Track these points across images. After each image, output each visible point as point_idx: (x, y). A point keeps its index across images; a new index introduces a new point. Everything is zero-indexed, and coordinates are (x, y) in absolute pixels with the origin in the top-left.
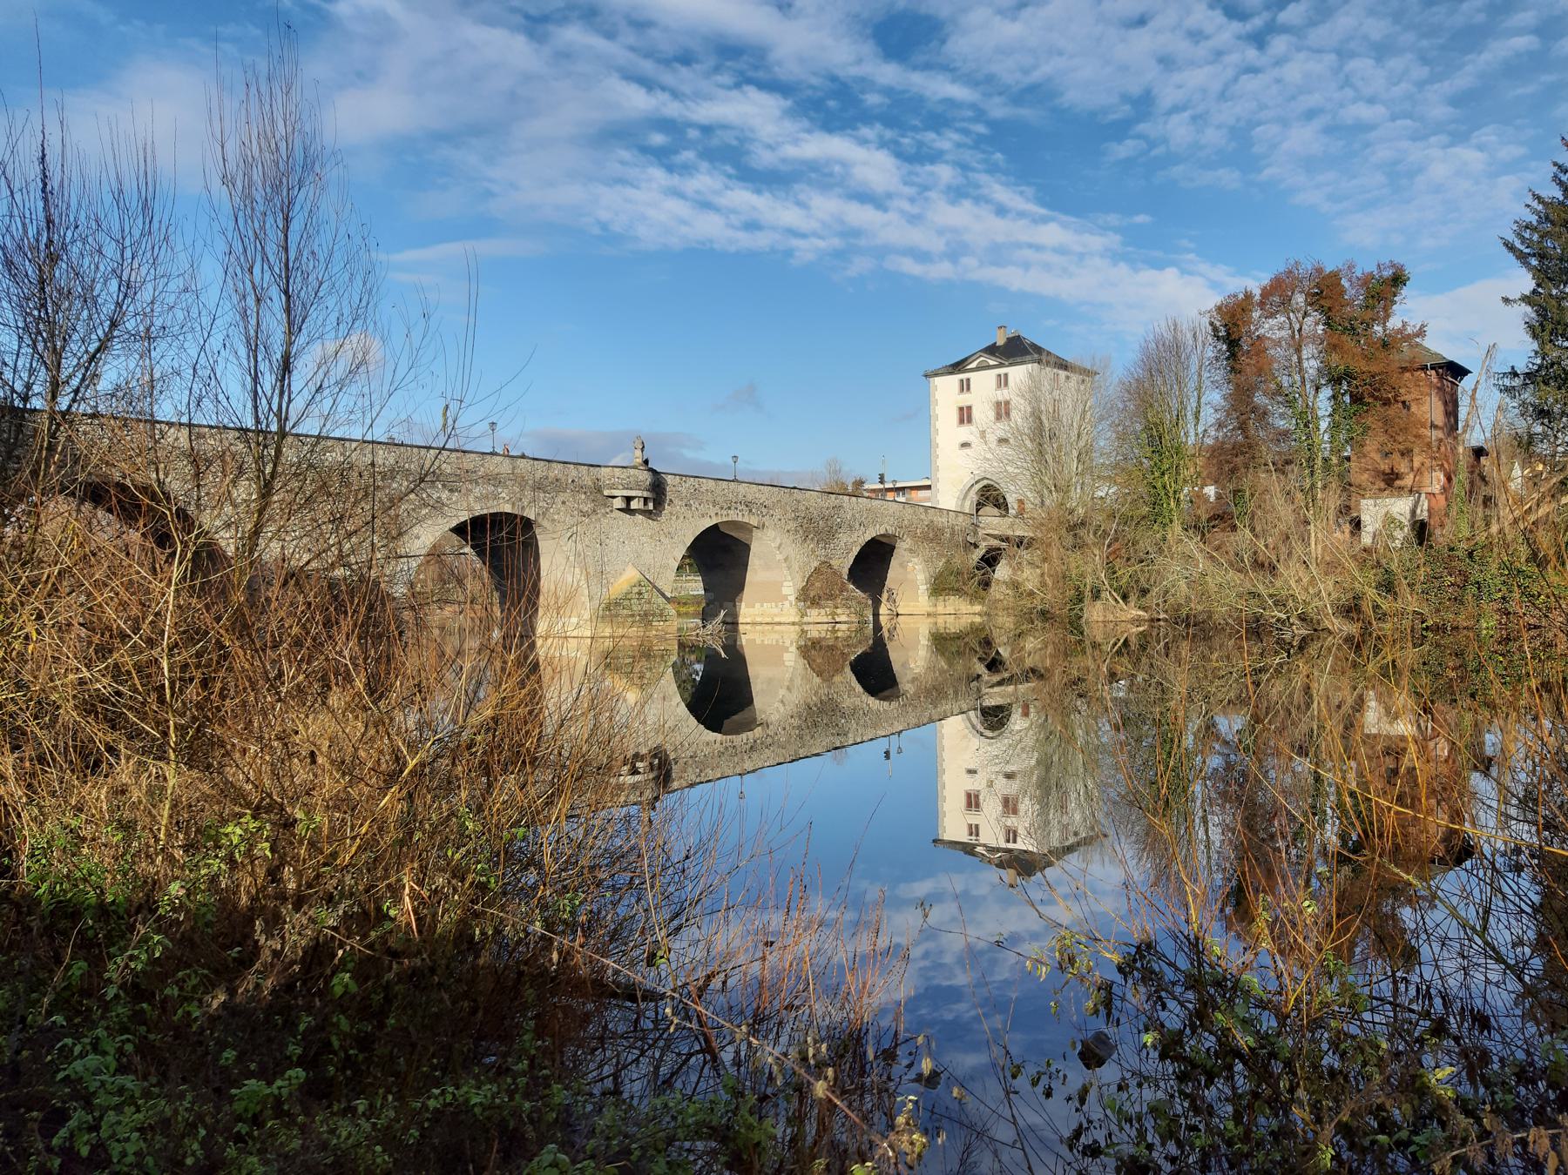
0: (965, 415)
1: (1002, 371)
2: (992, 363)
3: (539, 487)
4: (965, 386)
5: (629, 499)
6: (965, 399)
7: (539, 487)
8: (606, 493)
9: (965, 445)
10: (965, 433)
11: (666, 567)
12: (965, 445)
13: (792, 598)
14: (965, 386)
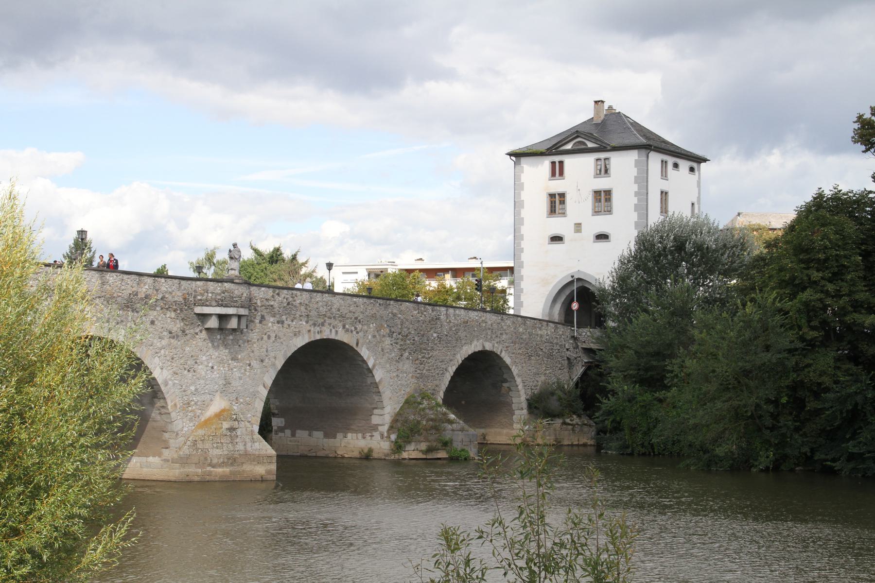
0: (556, 203)
1: (602, 155)
2: (590, 145)
3: (129, 305)
4: (557, 171)
5: (222, 318)
6: (557, 186)
7: (129, 305)
8: (198, 310)
9: (557, 239)
10: (557, 225)
11: (255, 395)
12: (557, 239)
13: (384, 429)
14: (557, 171)
